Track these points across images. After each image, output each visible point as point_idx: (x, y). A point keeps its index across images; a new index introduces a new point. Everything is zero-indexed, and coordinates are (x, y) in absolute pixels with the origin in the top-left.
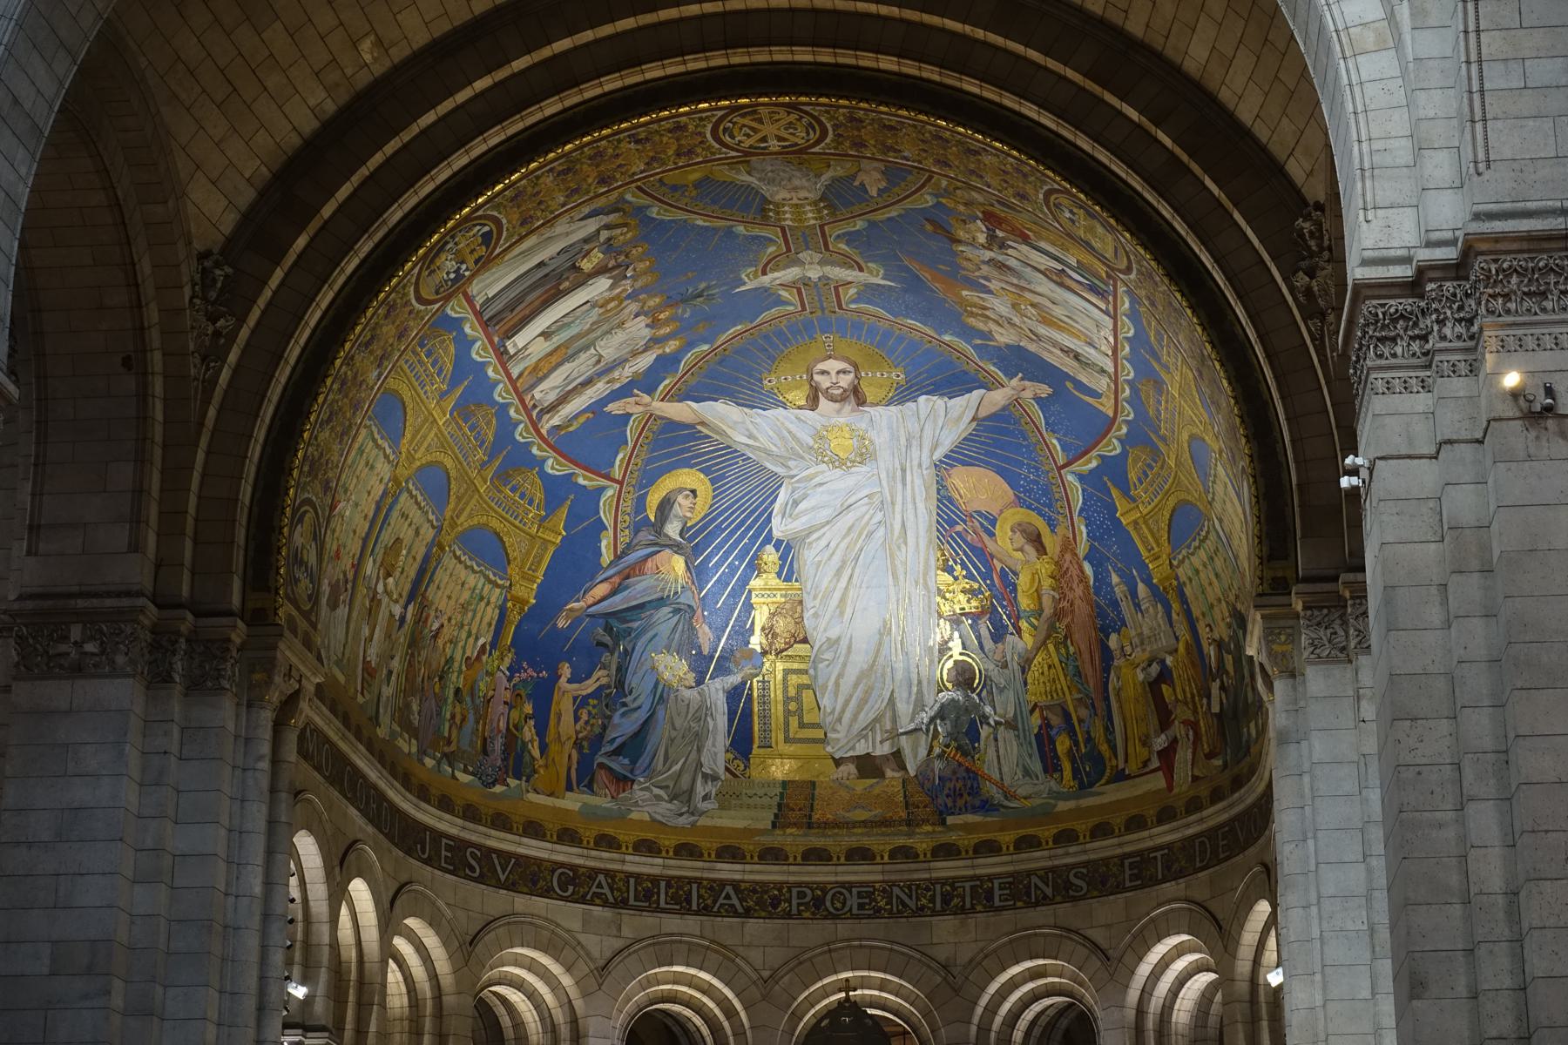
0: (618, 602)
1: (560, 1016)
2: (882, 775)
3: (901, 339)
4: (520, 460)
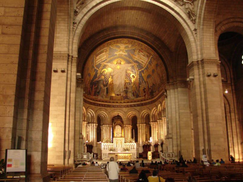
0: (98, 80)
1: (92, 115)
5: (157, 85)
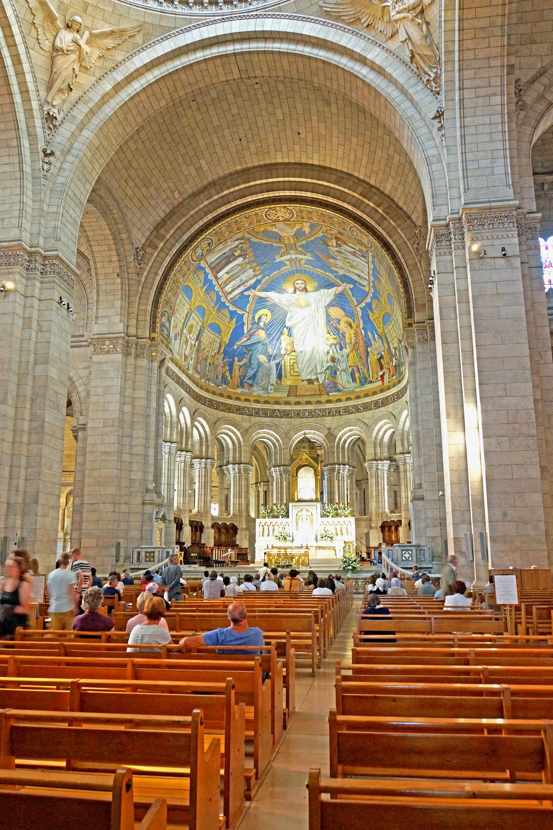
0: (249, 342)
1: (236, 441)
3: (316, 274)
4: (223, 306)
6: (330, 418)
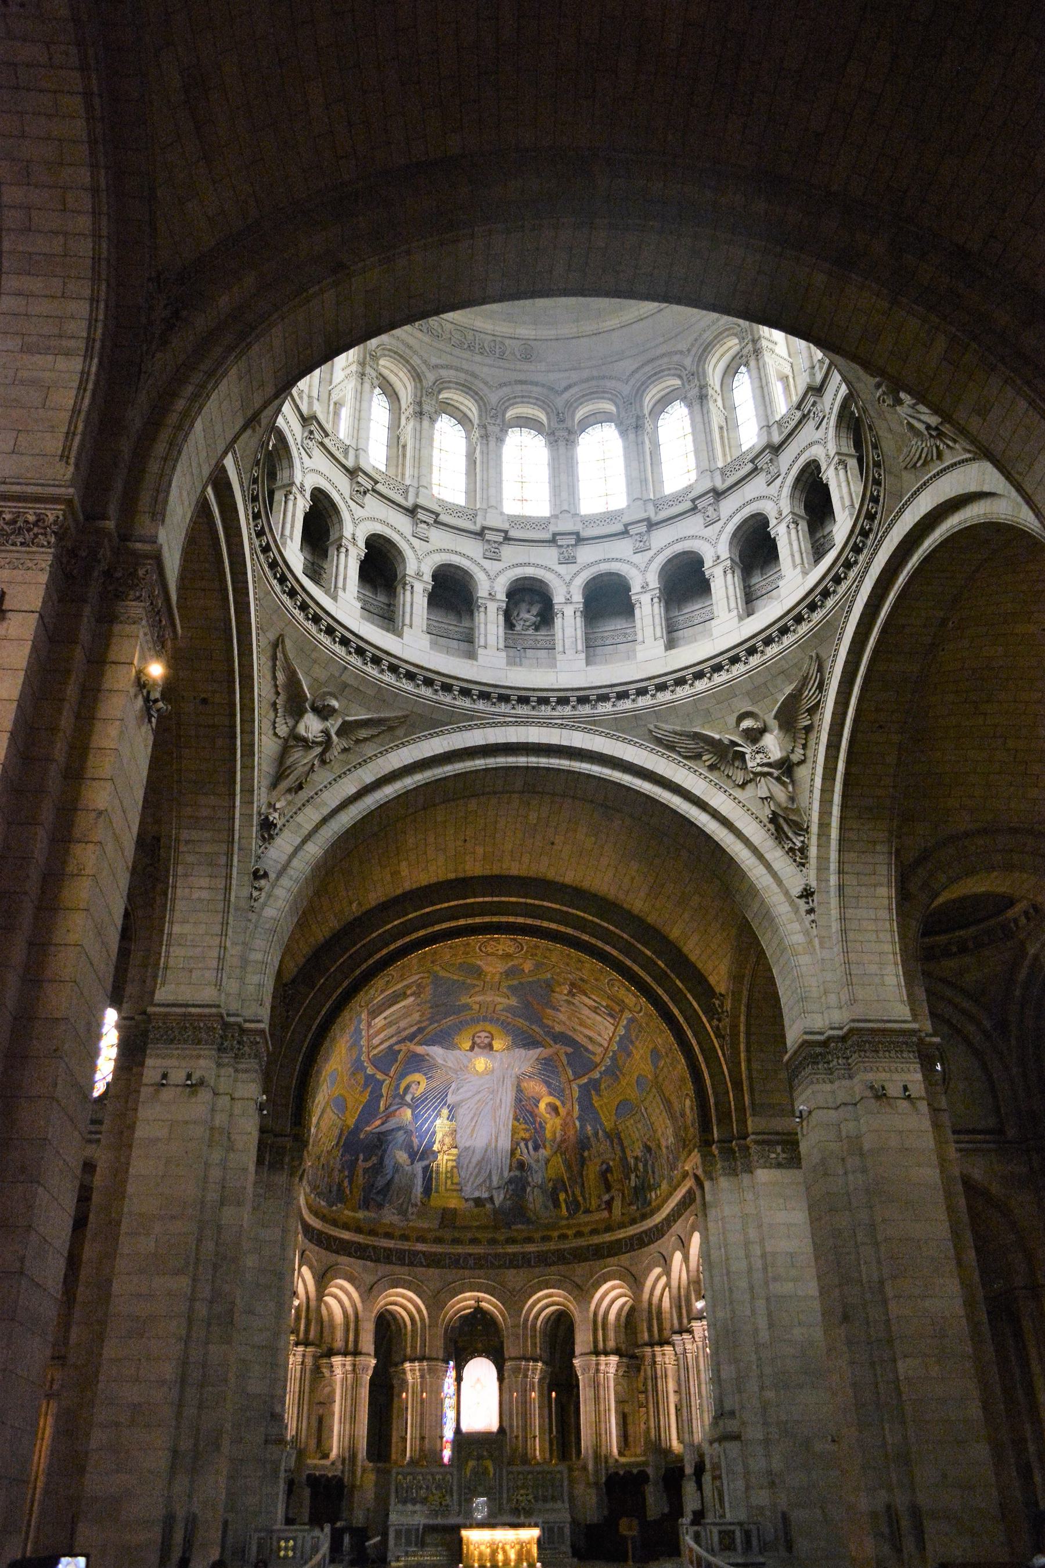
0: (384, 1128)
1: (350, 1311)
2: (484, 1206)
5: (664, 1150)
6: (513, 1271)
